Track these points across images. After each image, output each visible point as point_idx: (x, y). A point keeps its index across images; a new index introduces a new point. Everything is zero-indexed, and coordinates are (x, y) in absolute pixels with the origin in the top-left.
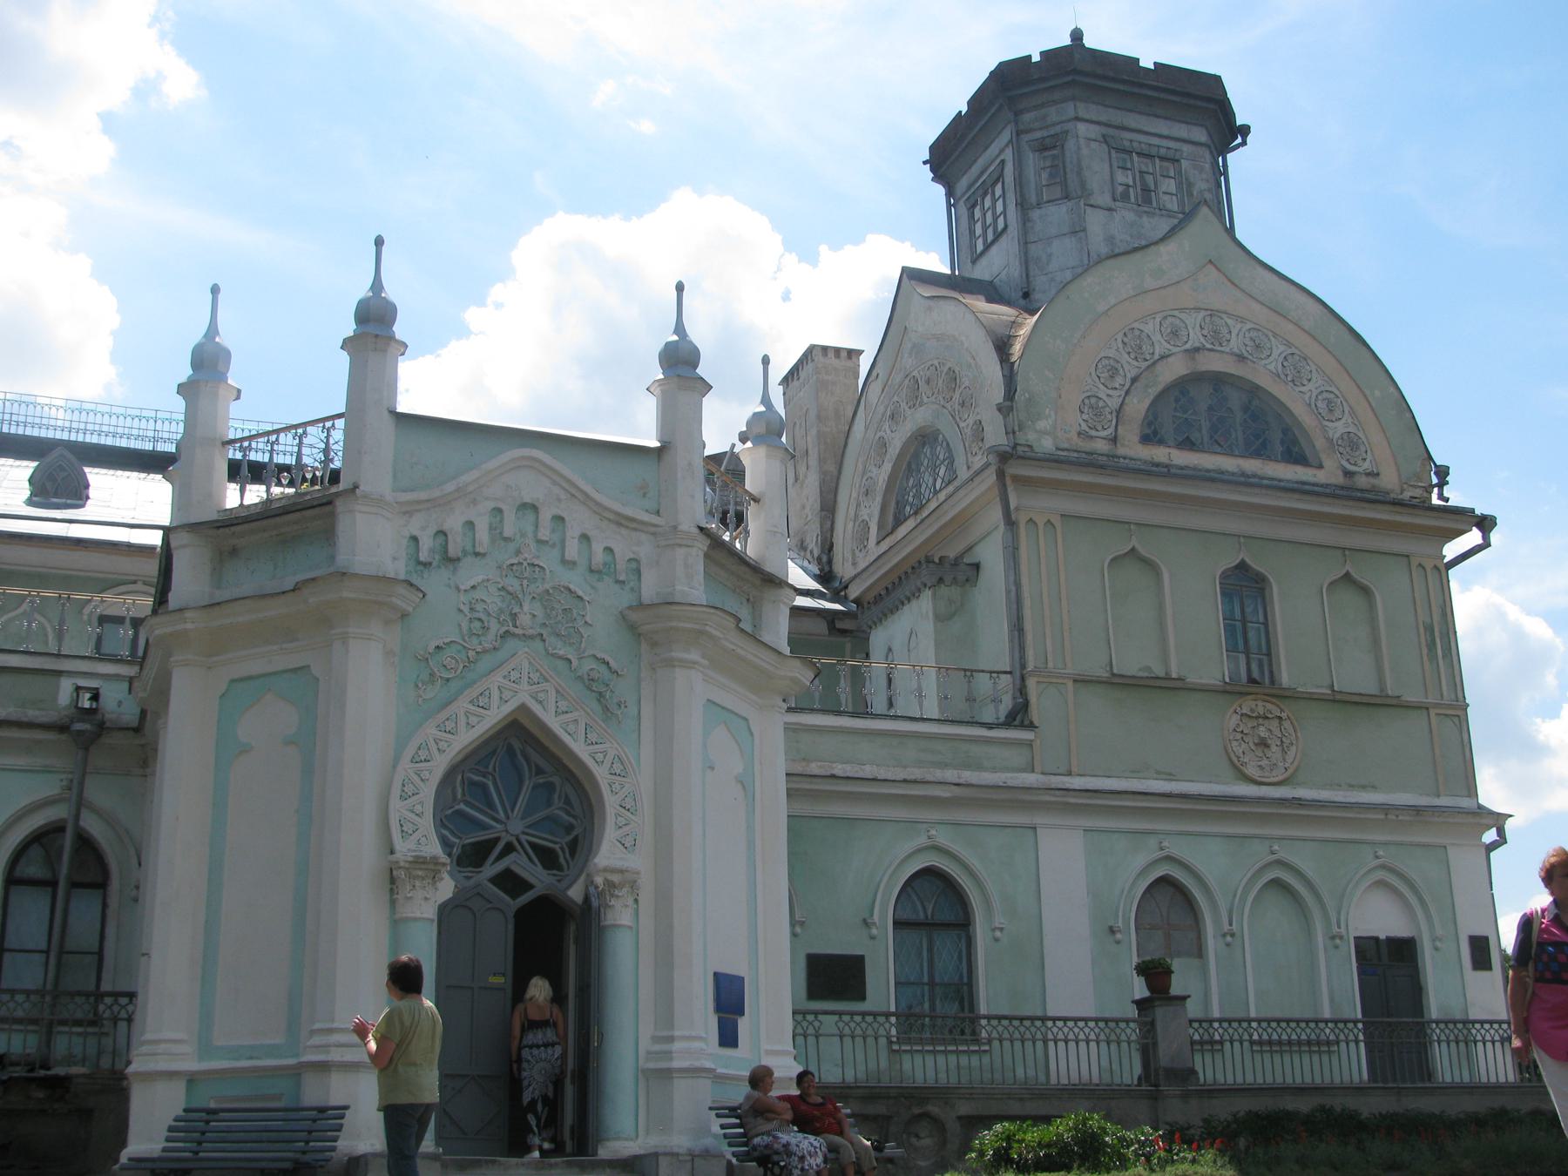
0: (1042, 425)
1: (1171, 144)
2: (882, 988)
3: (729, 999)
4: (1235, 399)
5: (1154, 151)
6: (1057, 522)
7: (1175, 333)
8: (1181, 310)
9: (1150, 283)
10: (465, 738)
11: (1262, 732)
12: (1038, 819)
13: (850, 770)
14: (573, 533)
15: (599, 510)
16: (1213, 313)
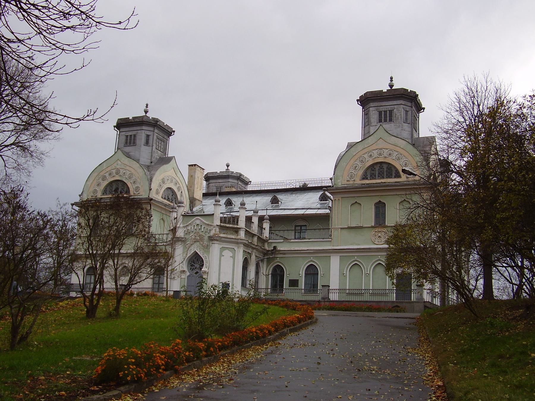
0: (339, 181)
1: (392, 107)
2: (302, 284)
4: (385, 166)
6: (340, 199)
7: (371, 156)
10: (189, 255)
11: (380, 235)
12: (331, 255)
14: (203, 227)
15: (206, 224)
16: (381, 149)
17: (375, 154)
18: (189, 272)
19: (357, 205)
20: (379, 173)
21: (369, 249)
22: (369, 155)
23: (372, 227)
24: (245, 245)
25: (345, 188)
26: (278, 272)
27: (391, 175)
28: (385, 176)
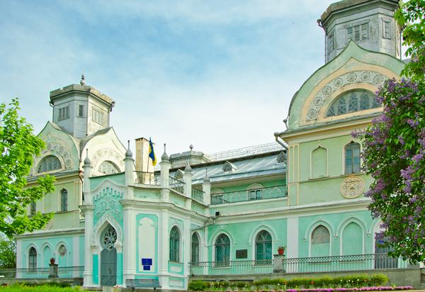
0: (296, 122)
3: (147, 263)
5: (359, 24)
6: (298, 145)
8: (342, 75)
9: (331, 71)
11: (352, 186)
13: (247, 213)
16: (353, 72)
17: (345, 80)
18: (103, 247)
19: (320, 150)
20: (350, 106)
21: (339, 205)
22: (336, 83)
23: (342, 177)
24: (170, 209)
25: (304, 130)
26: (223, 242)
27: (368, 105)
28: (359, 108)
